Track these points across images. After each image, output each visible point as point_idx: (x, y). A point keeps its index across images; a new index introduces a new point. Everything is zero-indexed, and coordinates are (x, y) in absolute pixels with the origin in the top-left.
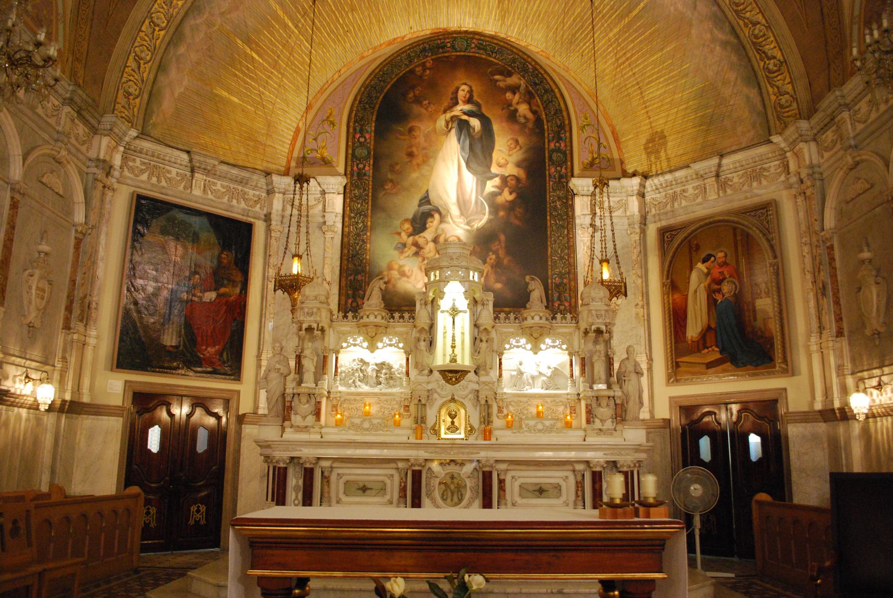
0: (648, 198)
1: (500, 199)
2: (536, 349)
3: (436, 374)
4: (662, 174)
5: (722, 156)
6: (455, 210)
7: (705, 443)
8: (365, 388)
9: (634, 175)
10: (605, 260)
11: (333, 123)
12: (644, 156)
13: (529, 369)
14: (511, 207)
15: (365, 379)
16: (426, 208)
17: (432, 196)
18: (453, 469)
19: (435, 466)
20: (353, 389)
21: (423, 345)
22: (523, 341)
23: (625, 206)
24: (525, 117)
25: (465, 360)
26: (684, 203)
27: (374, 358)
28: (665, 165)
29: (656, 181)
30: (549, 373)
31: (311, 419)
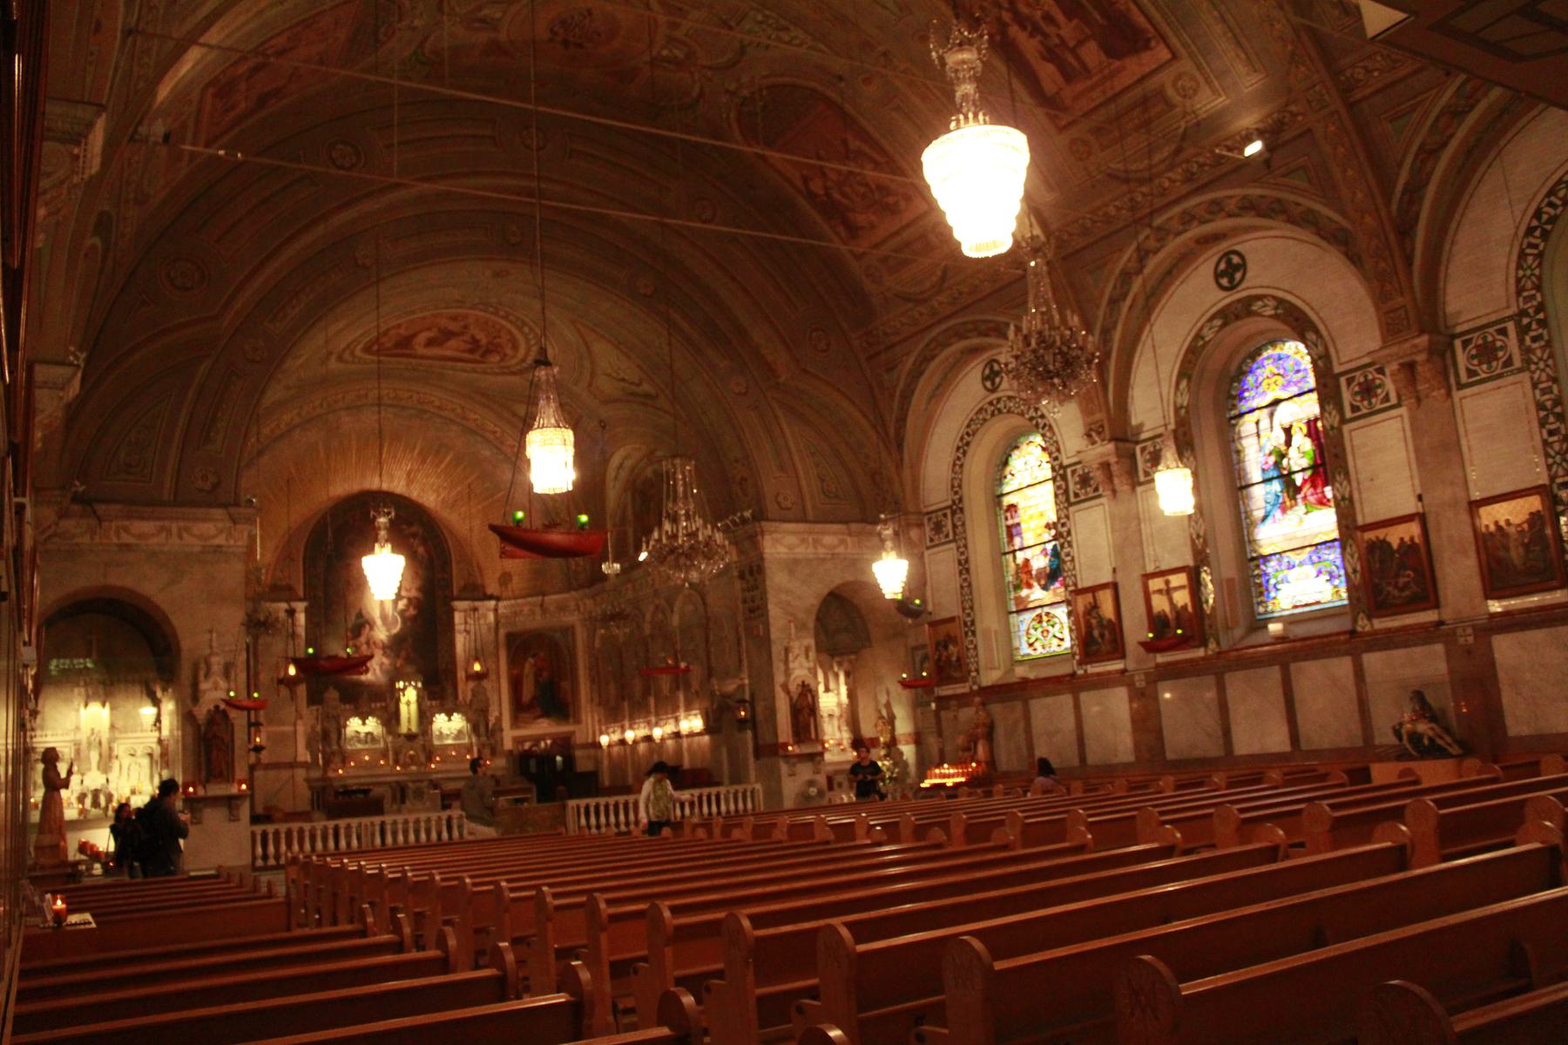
0: (500, 611)
1: (408, 614)
2: (450, 720)
3: (402, 738)
4: (509, 599)
5: (544, 595)
6: (379, 622)
7: (533, 763)
8: (360, 746)
9: (491, 598)
10: (477, 659)
11: (293, 560)
12: (497, 585)
13: (446, 732)
14: (414, 619)
15: (359, 741)
16: (361, 621)
17: (364, 612)
18: (417, 784)
19: (411, 785)
20: (354, 748)
21: (394, 722)
22: (443, 715)
23: (485, 616)
24: (423, 557)
25: (414, 729)
26: (522, 619)
27: (363, 730)
28: (510, 594)
29: (505, 603)
30: (455, 732)
31: (339, 765)
